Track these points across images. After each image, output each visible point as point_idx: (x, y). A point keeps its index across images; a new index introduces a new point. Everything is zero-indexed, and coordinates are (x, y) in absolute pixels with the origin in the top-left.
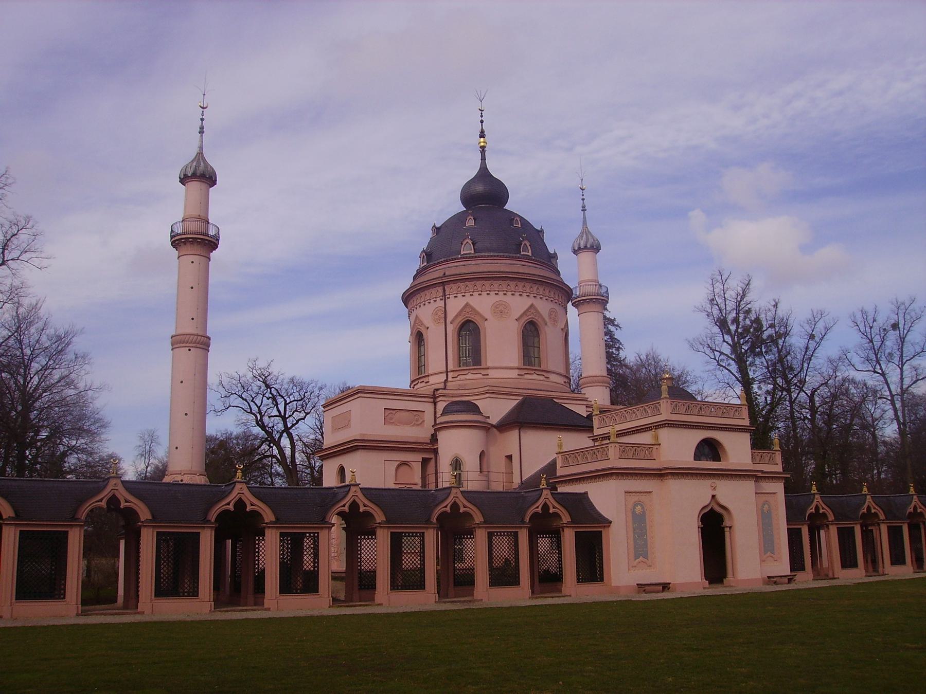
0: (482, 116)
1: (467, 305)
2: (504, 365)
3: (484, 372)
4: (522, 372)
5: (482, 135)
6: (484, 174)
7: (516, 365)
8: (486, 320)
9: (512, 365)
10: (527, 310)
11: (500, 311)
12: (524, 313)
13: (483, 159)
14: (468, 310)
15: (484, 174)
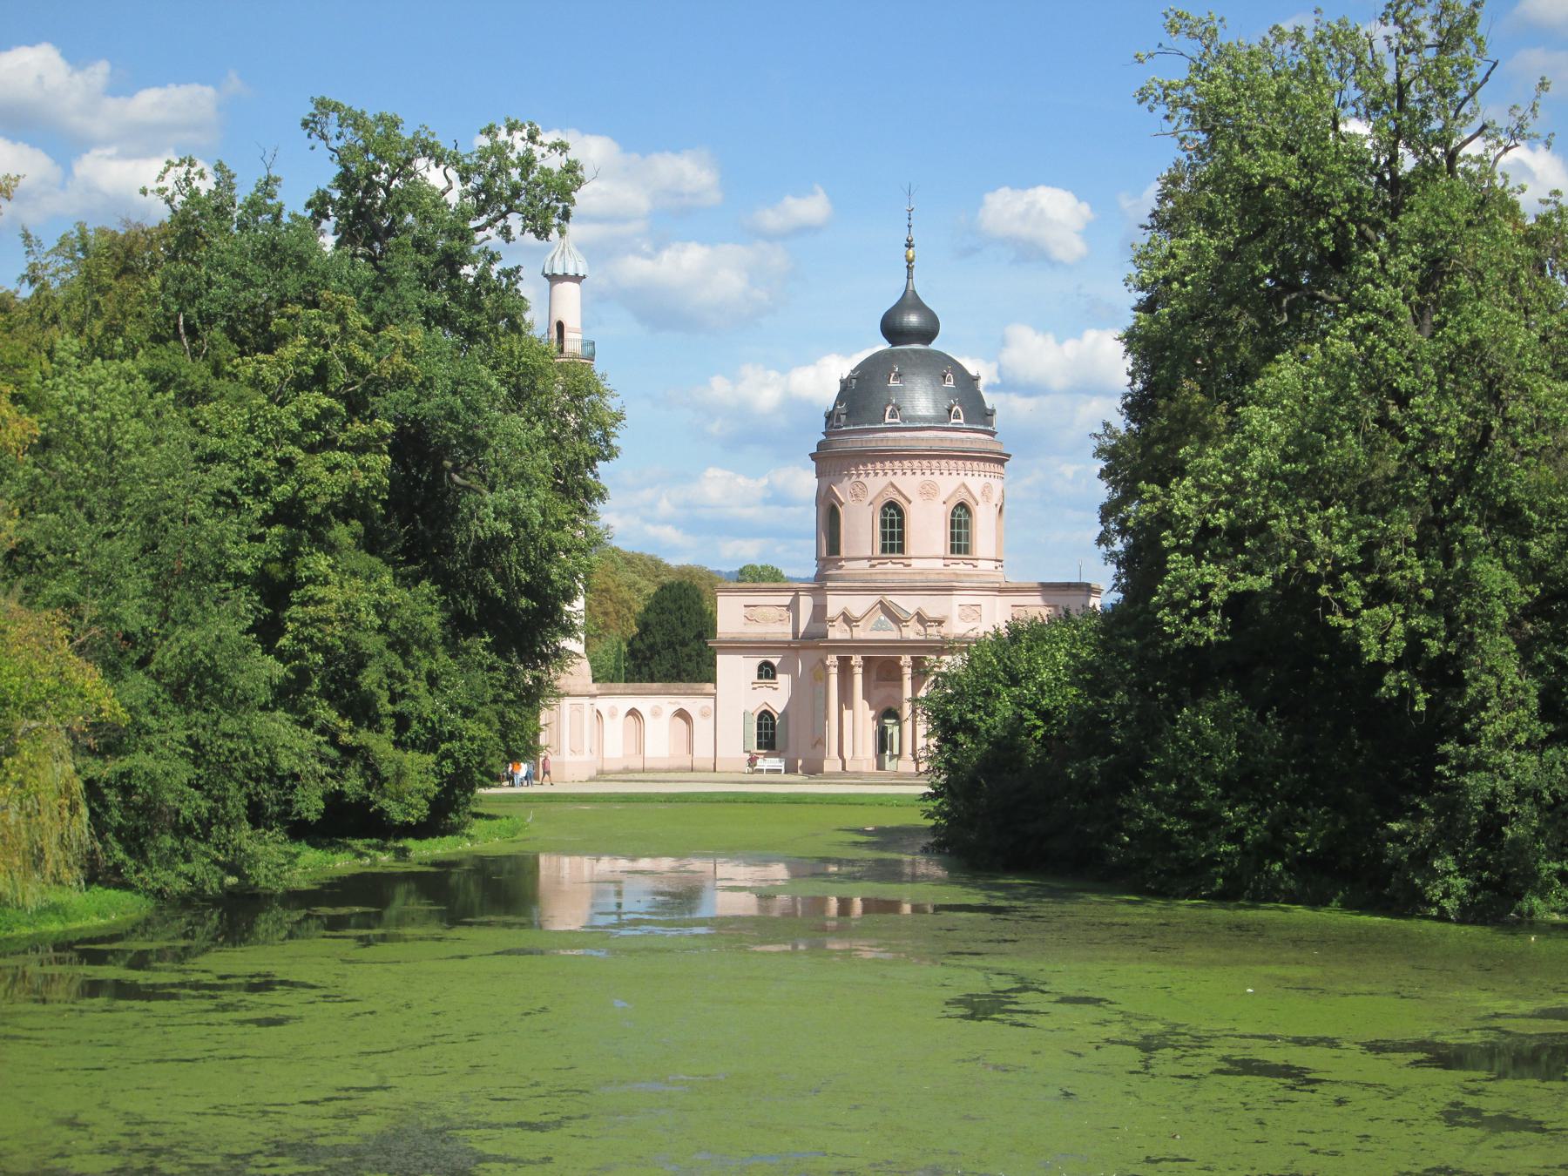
5: (909, 245)
7: (869, 554)
10: (885, 489)
12: (880, 494)
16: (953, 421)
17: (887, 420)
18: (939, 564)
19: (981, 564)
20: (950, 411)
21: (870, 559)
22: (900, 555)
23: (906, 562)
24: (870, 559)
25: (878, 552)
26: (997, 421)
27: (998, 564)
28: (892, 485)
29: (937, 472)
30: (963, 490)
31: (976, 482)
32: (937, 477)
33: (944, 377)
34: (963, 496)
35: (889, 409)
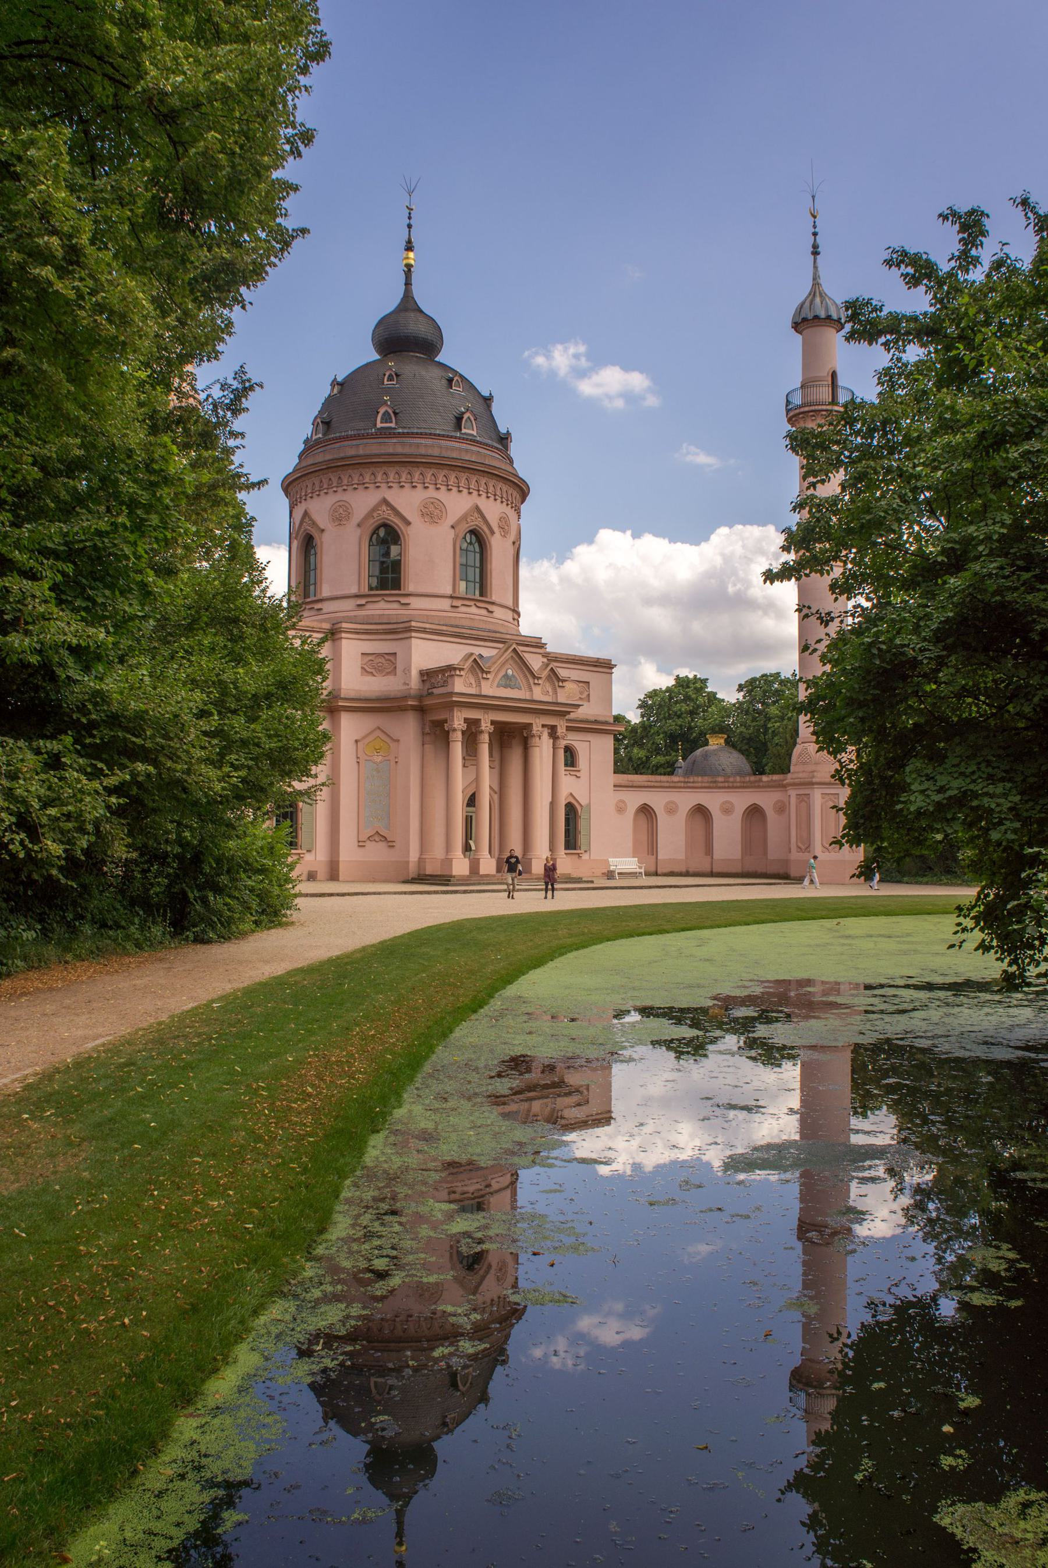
0: (410, 218)
1: (306, 514)
2: (339, 593)
3: (317, 606)
4: (362, 601)
5: (409, 248)
6: (408, 304)
7: (354, 590)
8: (323, 531)
9: (346, 592)
10: (375, 509)
11: (340, 516)
12: (370, 515)
13: (408, 283)
14: (307, 520)
15: (408, 304)
16: (464, 431)
17: (379, 425)
18: (446, 604)
19: (499, 613)
20: (459, 419)
21: (357, 596)
22: (397, 592)
23: (404, 600)
24: (357, 596)
25: (365, 590)
26: (515, 449)
27: (516, 617)
28: (385, 501)
29: (443, 488)
30: (476, 515)
31: (493, 510)
32: (442, 495)
33: (450, 381)
34: (476, 522)
35: (382, 411)
